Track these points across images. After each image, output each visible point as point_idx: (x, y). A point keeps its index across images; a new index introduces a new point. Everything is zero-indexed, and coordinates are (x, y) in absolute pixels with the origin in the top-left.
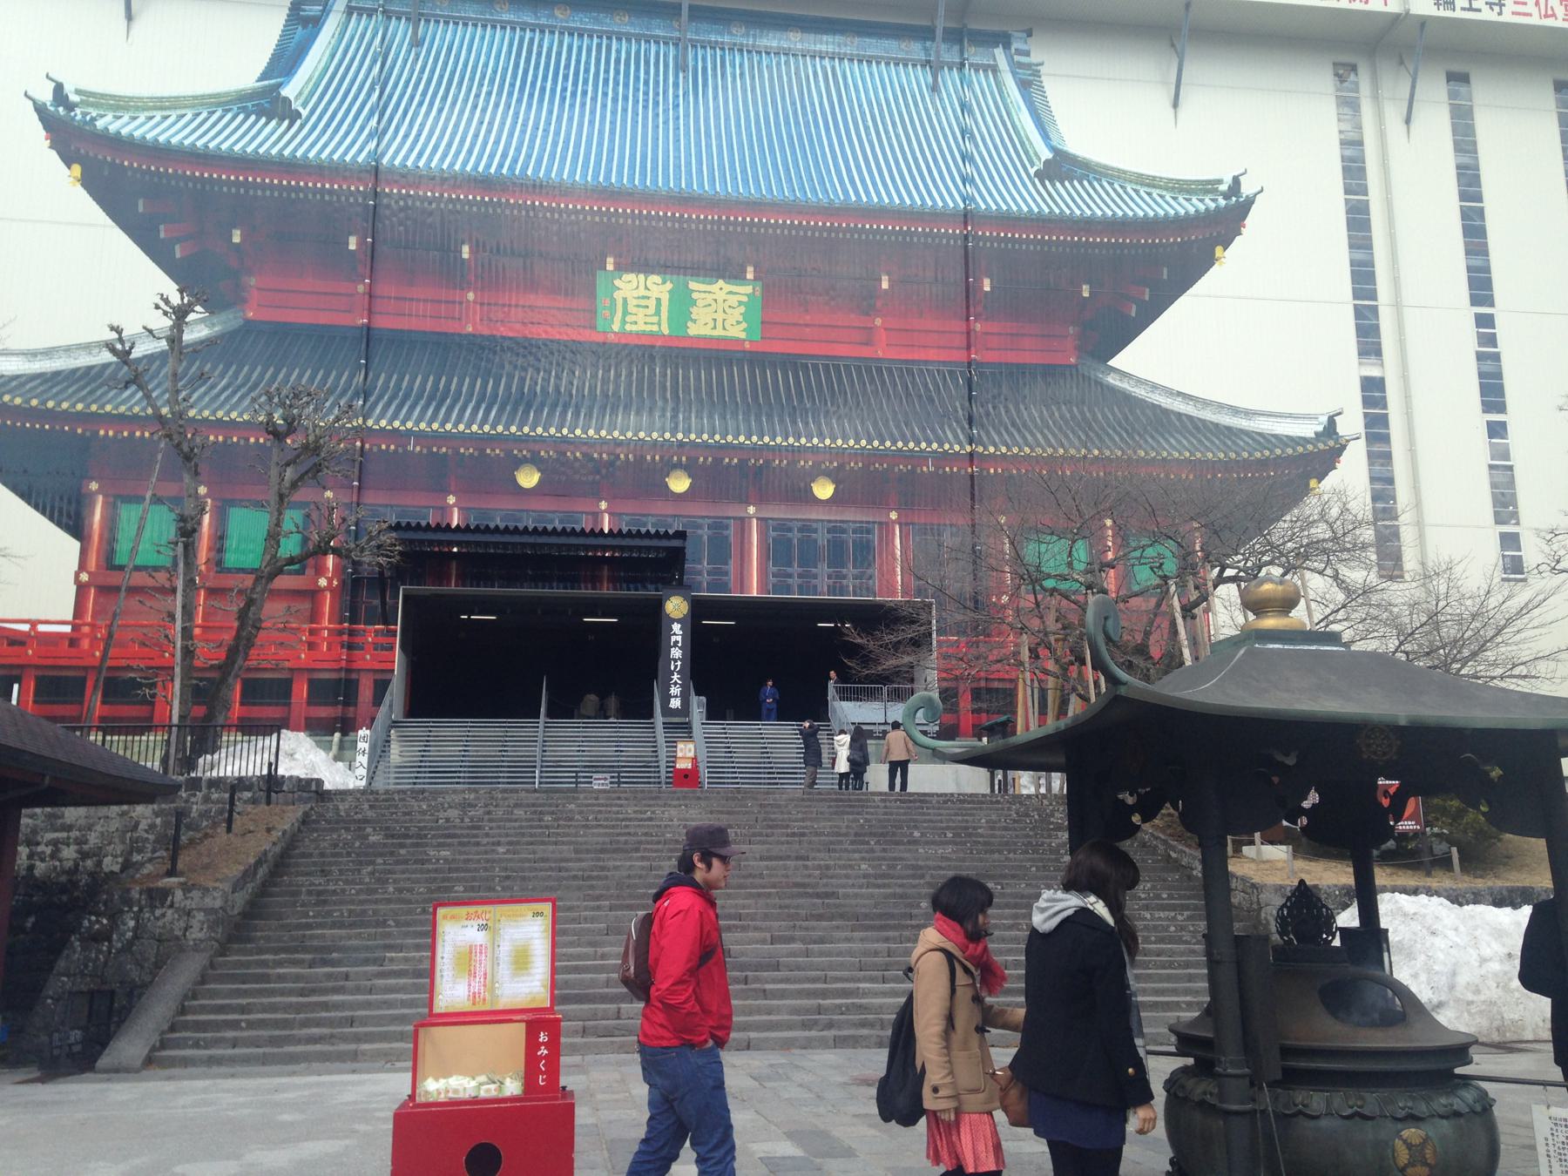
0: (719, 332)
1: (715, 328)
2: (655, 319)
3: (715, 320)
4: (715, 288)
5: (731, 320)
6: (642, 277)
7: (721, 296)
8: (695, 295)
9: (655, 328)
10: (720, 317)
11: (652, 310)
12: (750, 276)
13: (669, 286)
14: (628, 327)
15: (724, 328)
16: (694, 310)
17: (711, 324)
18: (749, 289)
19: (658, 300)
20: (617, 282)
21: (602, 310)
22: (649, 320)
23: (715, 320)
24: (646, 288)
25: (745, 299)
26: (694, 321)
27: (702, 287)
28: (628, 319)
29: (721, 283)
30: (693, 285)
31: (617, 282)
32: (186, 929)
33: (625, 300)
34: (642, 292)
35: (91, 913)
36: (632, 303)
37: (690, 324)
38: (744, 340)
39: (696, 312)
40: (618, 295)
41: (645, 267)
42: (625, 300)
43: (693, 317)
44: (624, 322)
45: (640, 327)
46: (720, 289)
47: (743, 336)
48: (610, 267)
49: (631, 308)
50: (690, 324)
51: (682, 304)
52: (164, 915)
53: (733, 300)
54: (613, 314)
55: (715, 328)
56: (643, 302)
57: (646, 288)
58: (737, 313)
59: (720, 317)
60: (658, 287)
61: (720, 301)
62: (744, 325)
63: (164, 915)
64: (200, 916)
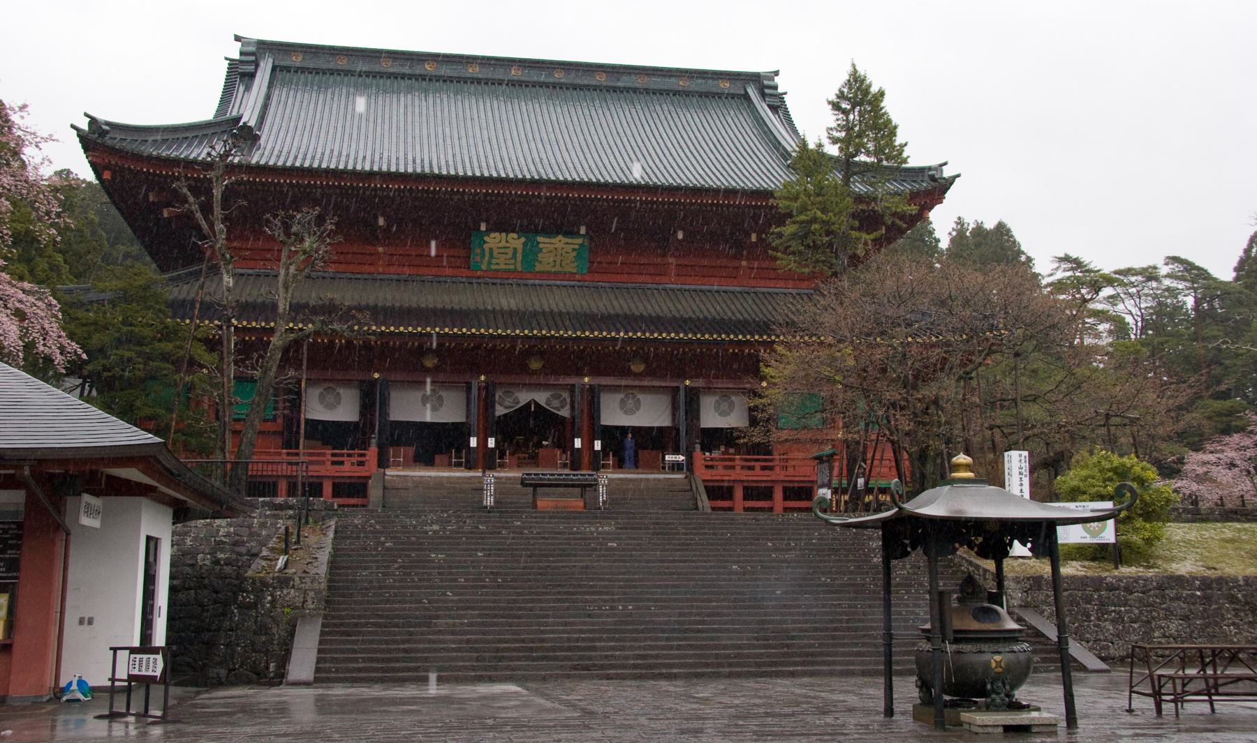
2: (513, 261)
4: (553, 240)
6: (504, 235)
8: (541, 246)
9: (512, 267)
11: (510, 255)
12: (583, 230)
13: (523, 240)
14: (494, 267)
17: (552, 264)
18: (580, 241)
20: (486, 238)
22: (507, 262)
24: (507, 241)
25: (577, 247)
26: (540, 262)
27: (547, 240)
28: (494, 261)
29: (560, 237)
30: (540, 239)
31: (486, 238)
32: (304, 603)
34: (503, 244)
35: (243, 592)
37: (536, 264)
41: (502, 226)
42: (491, 249)
44: (489, 263)
45: (502, 267)
46: (559, 241)
47: (575, 271)
49: (495, 254)
51: (531, 252)
52: (288, 593)
54: (483, 256)
56: (507, 250)
57: (507, 241)
60: (515, 241)
62: (576, 264)
63: (288, 593)
64: (312, 594)
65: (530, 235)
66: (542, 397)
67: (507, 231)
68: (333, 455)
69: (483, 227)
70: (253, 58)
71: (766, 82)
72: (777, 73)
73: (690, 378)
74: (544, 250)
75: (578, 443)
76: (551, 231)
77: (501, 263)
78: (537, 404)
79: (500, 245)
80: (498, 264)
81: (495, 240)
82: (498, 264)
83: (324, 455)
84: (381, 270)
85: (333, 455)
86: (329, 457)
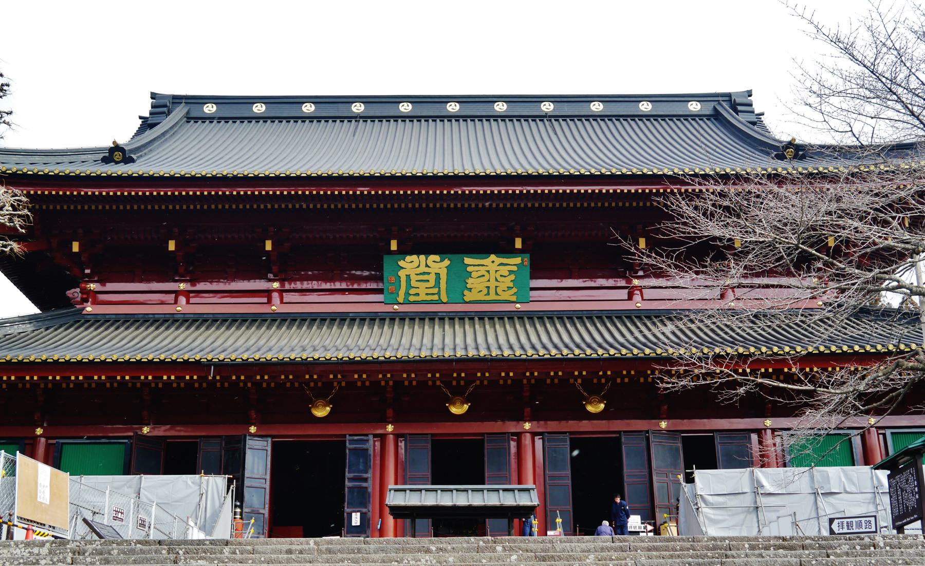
0: (492, 297)
1: (488, 294)
2: (435, 290)
3: (488, 287)
5: (502, 286)
6: (422, 257)
7: (493, 268)
8: (469, 269)
9: (436, 297)
10: (493, 284)
11: (432, 283)
12: (518, 244)
14: (412, 298)
15: (497, 294)
16: (470, 281)
17: (485, 291)
18: (518, 260)
19: (438, 275)
20: (401, 263)
23: (488, 287)
24: (427, 266)
25: (515, 268)
26: (470, 290)
28: (412, 291)
29: (493, 257)
30: (467, 261)
31: (401, 263)
33: (408, 276)
34: (423, 269)
36: (414, 278)
37: (466, 292)
40: (402, 274)
42: (408, 276)
43: (469, 286)
44: (407, 294)
45: (423, 297)
46: (492, 261)
48: (394, 245)
49: (413, 283)
50: (466, 292)
51: (459, 277)
53: (504, 270)
57: (427, 266)
59: (493, 284)
60: (437, 264)
62: (515, 290)
65: (456, 257)
67: (427, 252)
69: (394, 245)
70: (165, 109)
71: (738, 100)
72: (750, 94)
73: (668, 417)
74: (473, 275)
76: (482, 249)
77: (423, 291)
80: (418, 294)
81: (411, 264)
82: (418, 294)
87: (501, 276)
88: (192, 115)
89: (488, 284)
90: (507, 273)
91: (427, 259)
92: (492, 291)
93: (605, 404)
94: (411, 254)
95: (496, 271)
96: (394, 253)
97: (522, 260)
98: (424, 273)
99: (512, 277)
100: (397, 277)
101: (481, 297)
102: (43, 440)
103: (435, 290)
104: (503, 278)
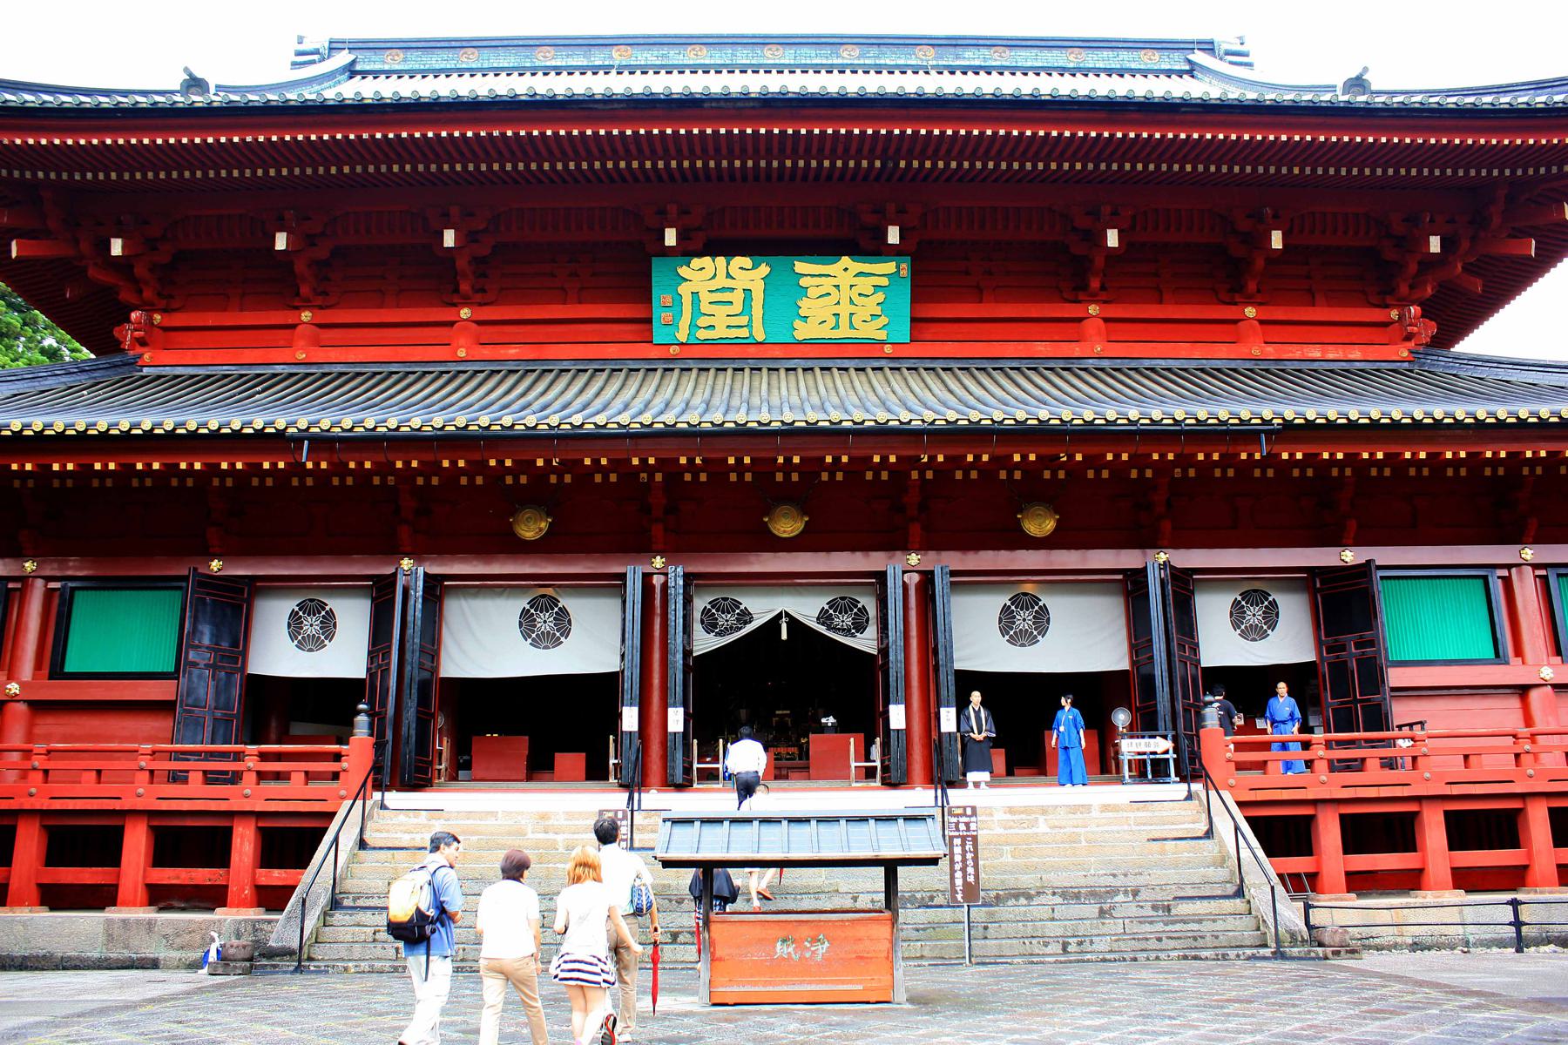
0: (844, 332)
1: (836, 327)
2: (744, 320)
6: (721, 260)
7: (845, 280)
8: (804, 282)
9: (744, 333)
10: (845, 310)
11: (737, 308)
12: (893, 236)
14: (703, 335)
15: (851, 326)
18: (889, 267)
21: (659, 314)
24: (728, 276)
25: (884, 281)
28: (703, 322)
30: (801, 266)
31: (683, 271)
34: (722, 281)
36: (705, 298)
37: (798, 323)
38: (883, 343)
39: (806, 306)
40: (685, 290)
43: (802, 312)
44: (693, 326)
45: (720, 332)
47: (881, 335)
48: (670, 238)
49: (705, 308)
50: (798, 323)
51: (785, 293)
53: (866, 285)
55: (836, 327)
57: (728, 276)
58: (871, 305)
59: (845, 310)
60: (747, 273)
61: (845, 287)
62: (884, 320)
66: (807, 608)
68: (264, 757)
69: (670, 238)
75: (897, 717)
76: (827, 247)
77: (720, 326)
78: (794, 623)
79: (715, 285)
81: (702, 274)
83: (238, 756)
84: (462, 353)
85: (264, 757)
86: (251, 763)
87: (860, 294)
88: (358, 67)
89: (836, 309)
90: (871, 290)
91: (728, 264)
92: (844, 320)
93: (1058, 521)
94: (700, 255)
95: (852, 286)
96: (669, 252)
97: (898, 267)
98: (723, 289)
99: (880, 297)
100: (677, 296)
101: (825, 333)
102: (39, 583)
103: (744, 320)
104: (862, 298)
